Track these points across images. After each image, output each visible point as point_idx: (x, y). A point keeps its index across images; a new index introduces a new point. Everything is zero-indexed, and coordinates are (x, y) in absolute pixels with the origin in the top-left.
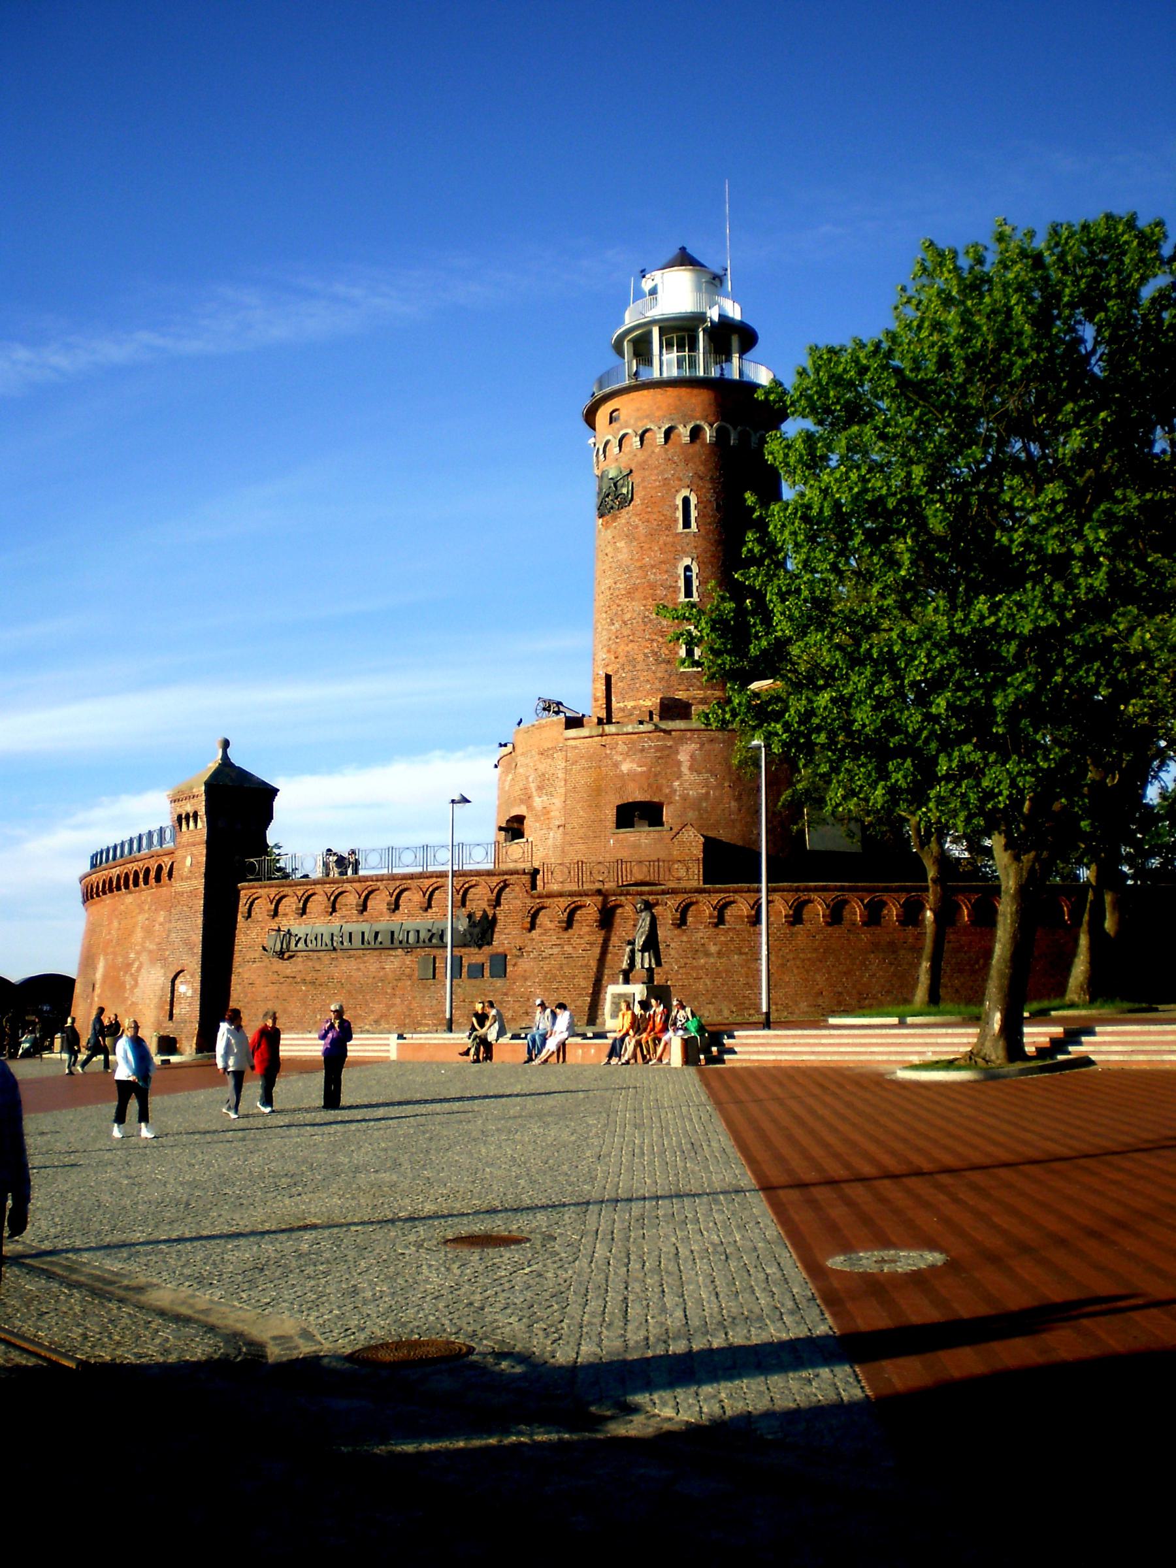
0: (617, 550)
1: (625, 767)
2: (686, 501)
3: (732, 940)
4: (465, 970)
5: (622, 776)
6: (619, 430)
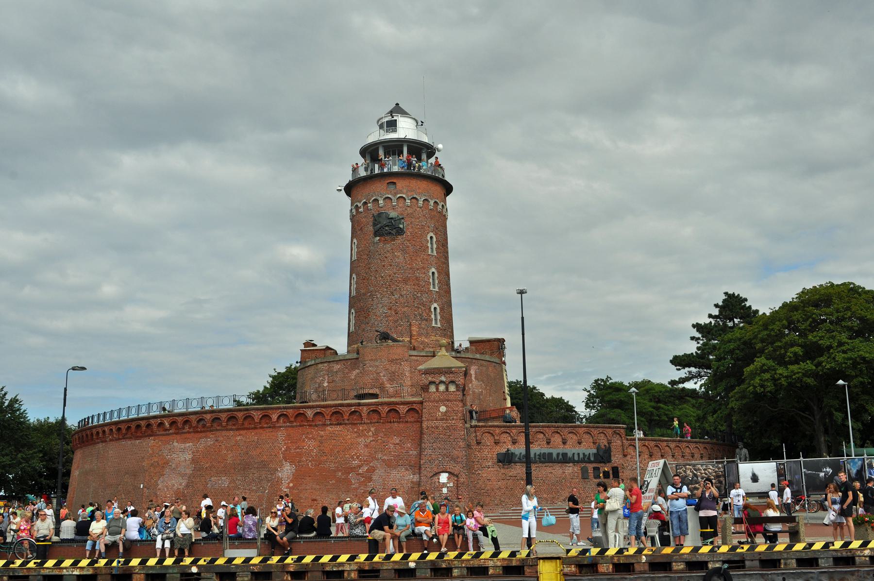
6: (396, 194)
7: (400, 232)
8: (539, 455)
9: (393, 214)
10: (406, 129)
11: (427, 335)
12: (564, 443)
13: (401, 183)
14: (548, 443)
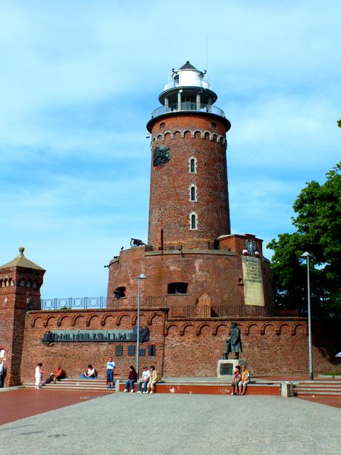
0: (164, 180)
1: (172, 268)
2: (193, 160)
3: (254, 341)
4: (137, 352)
5: (170, 272)
6: (164, 131)
7: (167, 160)
8: (78, 336)
9: (162, 148)
10: (189, 80)
11: (184, 238)
12: (103, 324)
13: (168, 122)
14: (88, 324)
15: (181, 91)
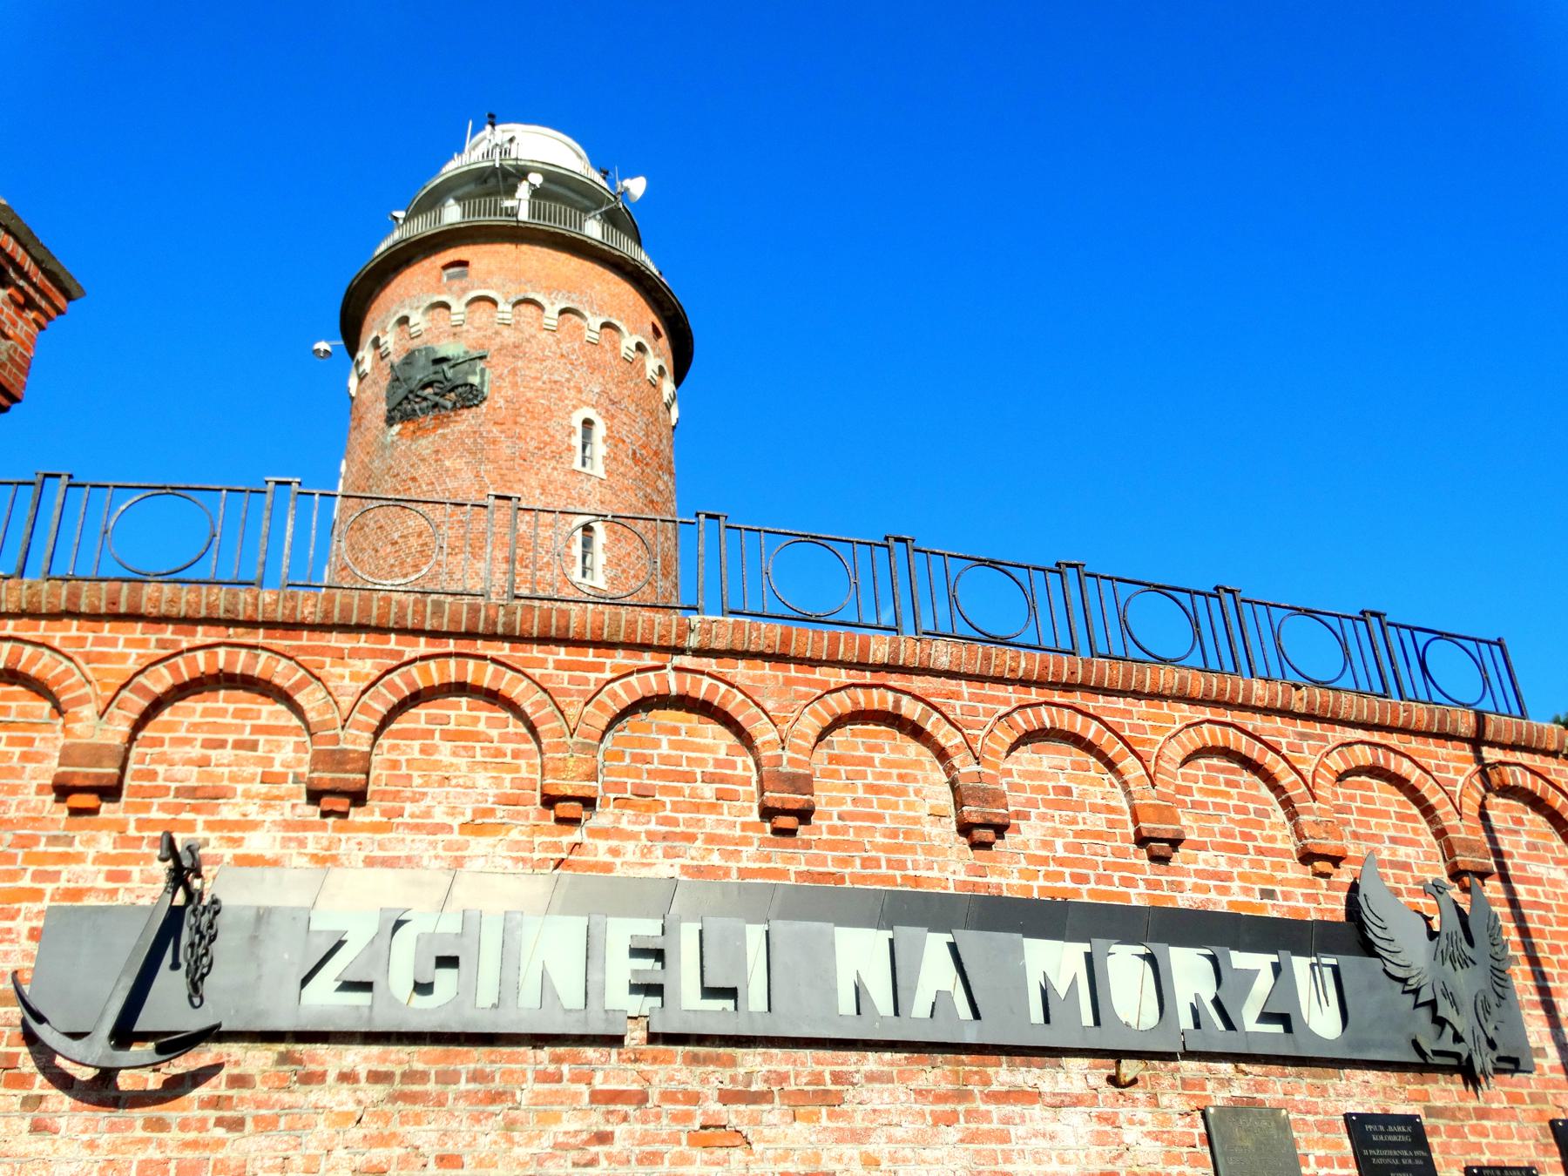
2: (588, 423)
6: (464, 291)
7: (471, 397)
15: (536, 179)
